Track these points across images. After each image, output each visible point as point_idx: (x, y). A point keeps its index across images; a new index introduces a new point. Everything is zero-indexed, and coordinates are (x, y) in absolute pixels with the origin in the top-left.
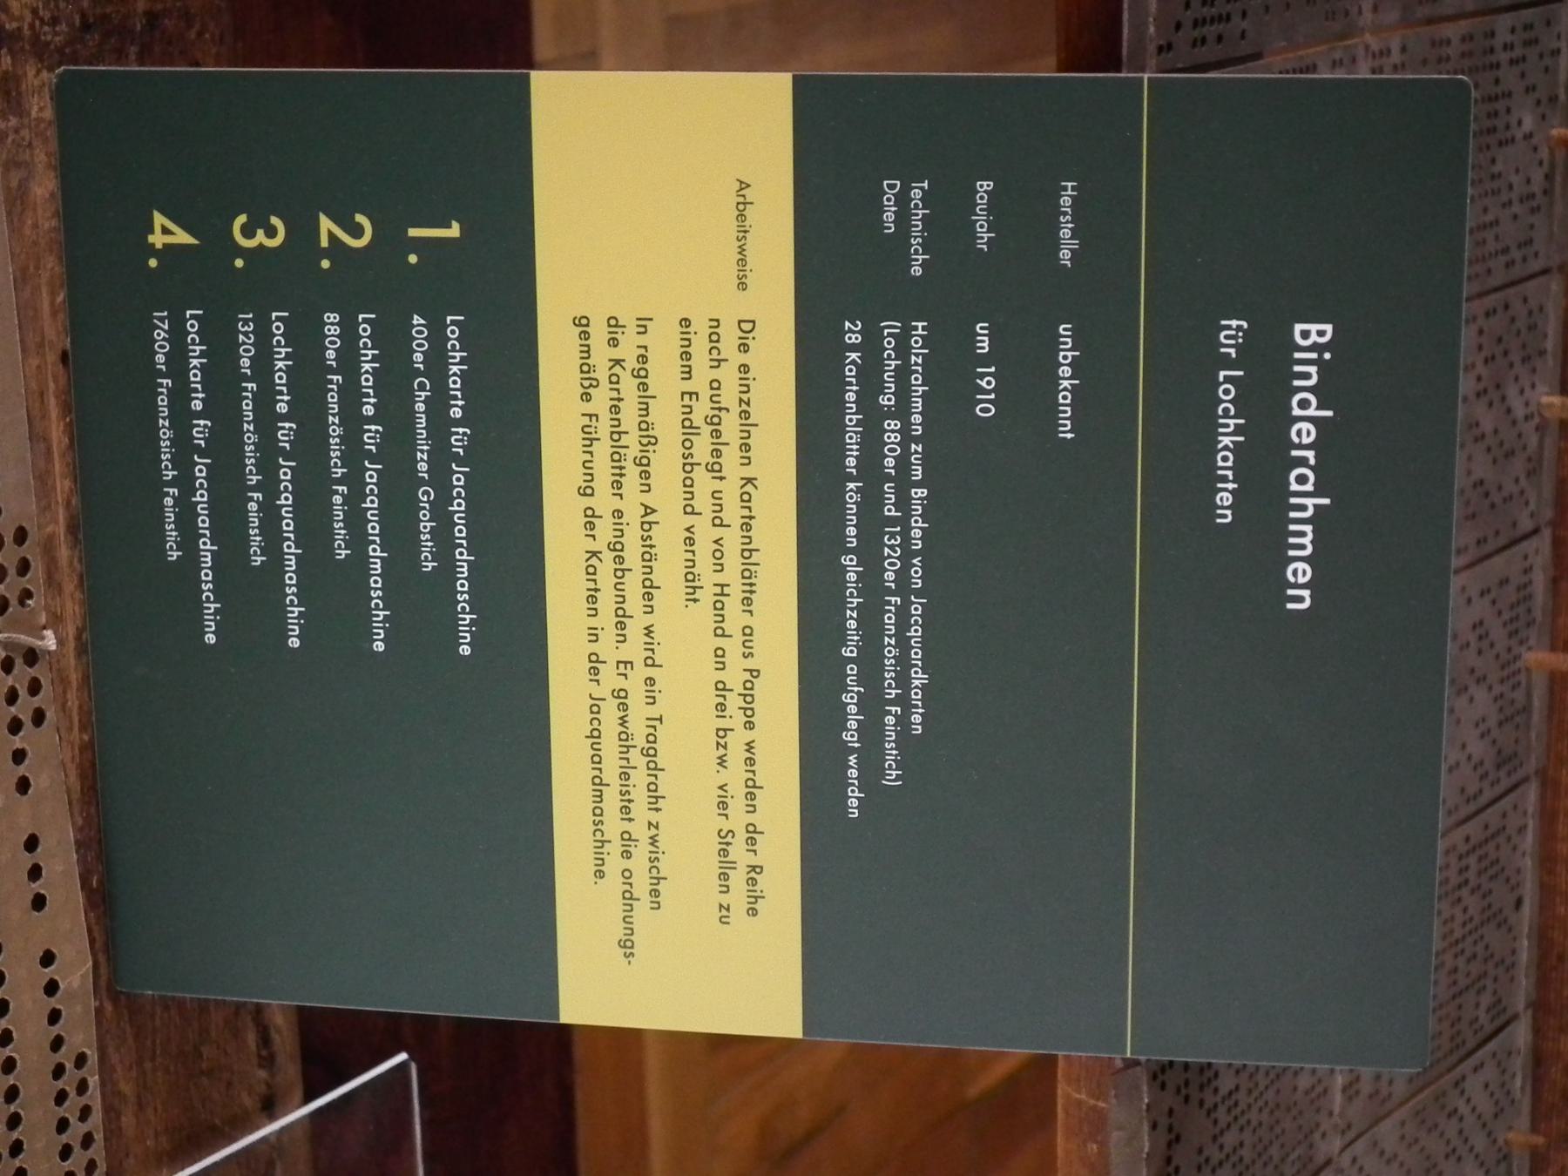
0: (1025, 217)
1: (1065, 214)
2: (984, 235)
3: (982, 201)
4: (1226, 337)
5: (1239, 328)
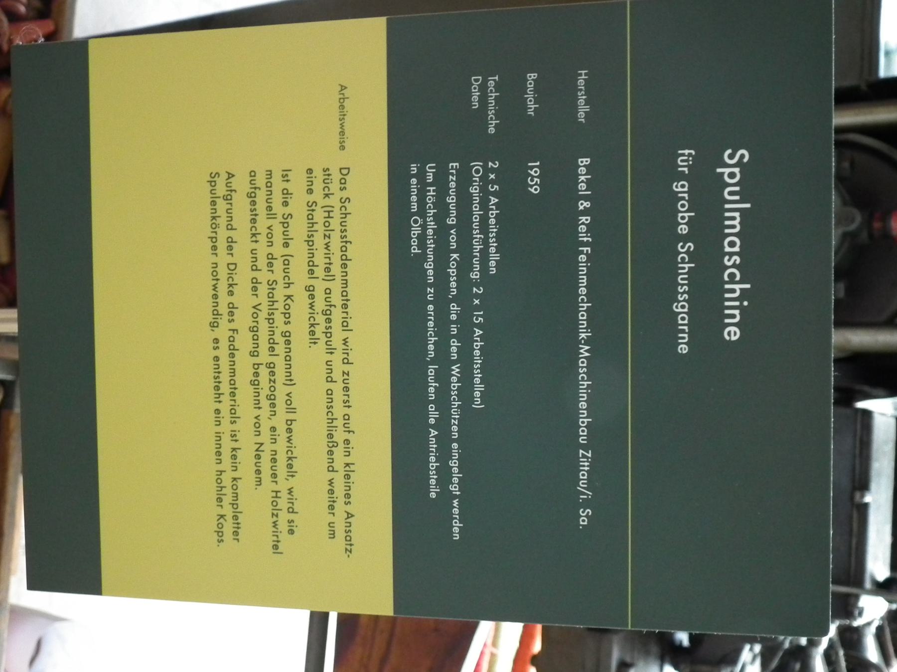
0: (556, 92)
1: (581, 90)
3: (530, 86)
4: (682, 161)
5: (690, 155)
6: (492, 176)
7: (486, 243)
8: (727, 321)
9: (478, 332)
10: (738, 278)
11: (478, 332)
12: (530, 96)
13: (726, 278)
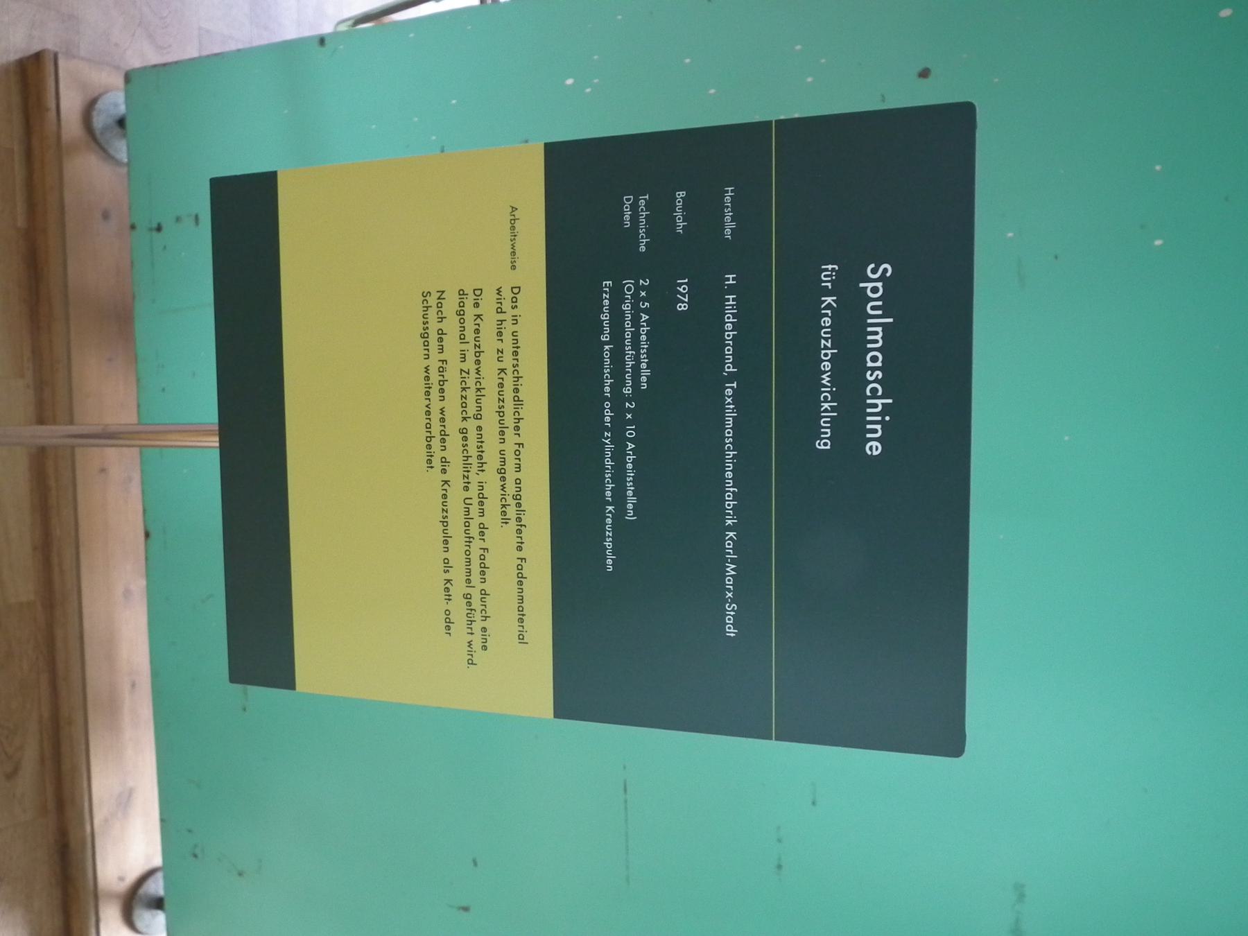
0: (704, 212)
2: (681, 224)
3: (679, 205)
5: (833, 270)
6: (643, 294)
7: (637, 358)
8: (869, 436)
9: (631, 446)
10: (880, 393)
11: (631, 446)
12: (679, 214)
13: (868, 393)
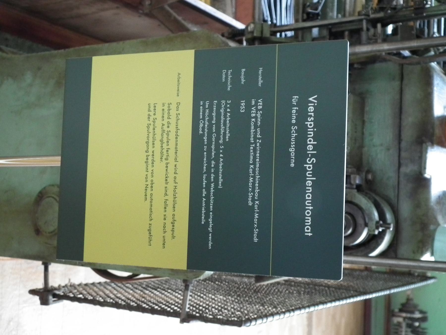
0: (252, 76)
3: (243, 74)
5: (297, 98)
6: (228, 106)
7: (225, 130)
9: (221, 160)
11: (221, 160)
12: (242, 77)
